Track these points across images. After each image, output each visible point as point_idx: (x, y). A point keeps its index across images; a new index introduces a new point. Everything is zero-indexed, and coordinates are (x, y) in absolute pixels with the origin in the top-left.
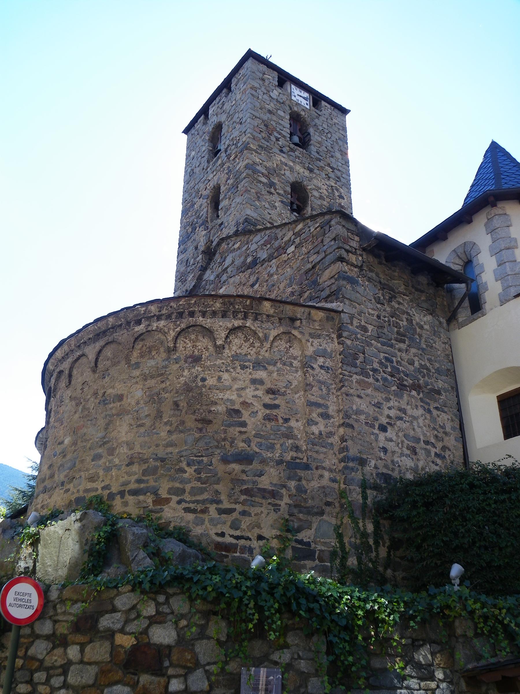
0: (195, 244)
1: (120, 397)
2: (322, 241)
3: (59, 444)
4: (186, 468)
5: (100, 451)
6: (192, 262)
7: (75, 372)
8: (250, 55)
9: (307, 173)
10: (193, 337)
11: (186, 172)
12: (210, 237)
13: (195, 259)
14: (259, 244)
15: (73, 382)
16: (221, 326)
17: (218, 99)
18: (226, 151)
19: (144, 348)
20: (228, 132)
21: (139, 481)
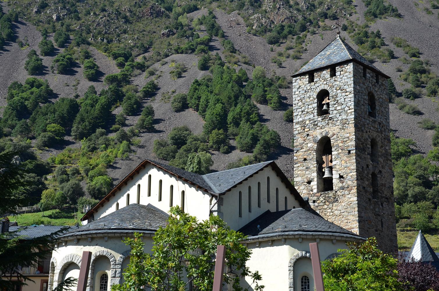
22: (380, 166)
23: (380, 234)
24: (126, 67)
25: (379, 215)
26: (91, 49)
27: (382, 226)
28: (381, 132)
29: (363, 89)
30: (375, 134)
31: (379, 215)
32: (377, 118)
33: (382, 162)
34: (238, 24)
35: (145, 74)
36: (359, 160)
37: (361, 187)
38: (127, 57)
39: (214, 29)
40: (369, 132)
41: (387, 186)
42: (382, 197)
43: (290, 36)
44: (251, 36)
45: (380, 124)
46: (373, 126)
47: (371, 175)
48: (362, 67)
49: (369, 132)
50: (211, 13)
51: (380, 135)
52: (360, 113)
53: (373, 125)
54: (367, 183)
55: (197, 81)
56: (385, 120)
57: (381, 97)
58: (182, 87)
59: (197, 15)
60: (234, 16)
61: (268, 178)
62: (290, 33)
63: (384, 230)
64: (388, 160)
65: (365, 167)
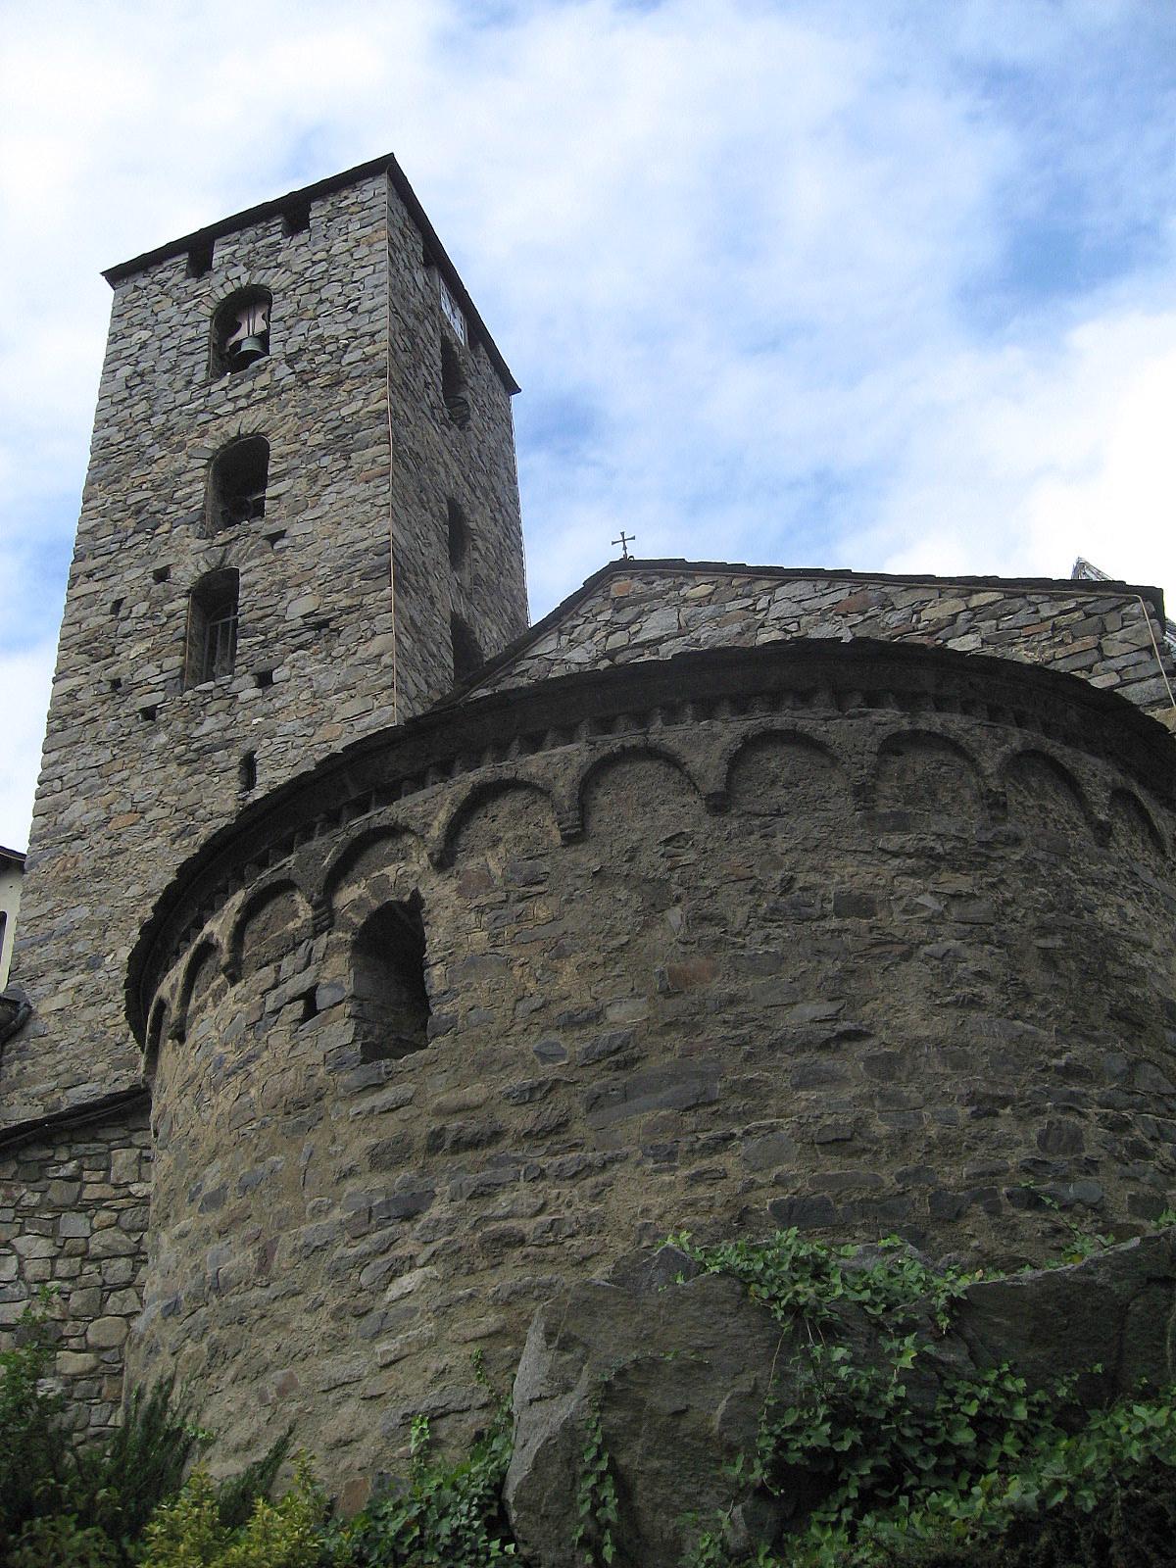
0: (159, 565)
1: (858, 905)
2: (1099, 648)
3: (571, 1022)
4: (1151, 1145)
5: (826, 1061)
6: (142, 608)
7: (602, 798)
8: (387, 166)
9: (467, 490)
10: (1034, 782)
11: (109, 372)
12: (223, 558)
13: (158, 603)
14: (806, 604)
15: (594, 826)
16: (1096, 773)
17: (251, 233)
18: (291, 360)
19: (910, 779)
20: (298, 315)
21: (1032, 1167)
30: (249, 421)
33: (302, 485)
36: (98, 586)
56: (350, 315)
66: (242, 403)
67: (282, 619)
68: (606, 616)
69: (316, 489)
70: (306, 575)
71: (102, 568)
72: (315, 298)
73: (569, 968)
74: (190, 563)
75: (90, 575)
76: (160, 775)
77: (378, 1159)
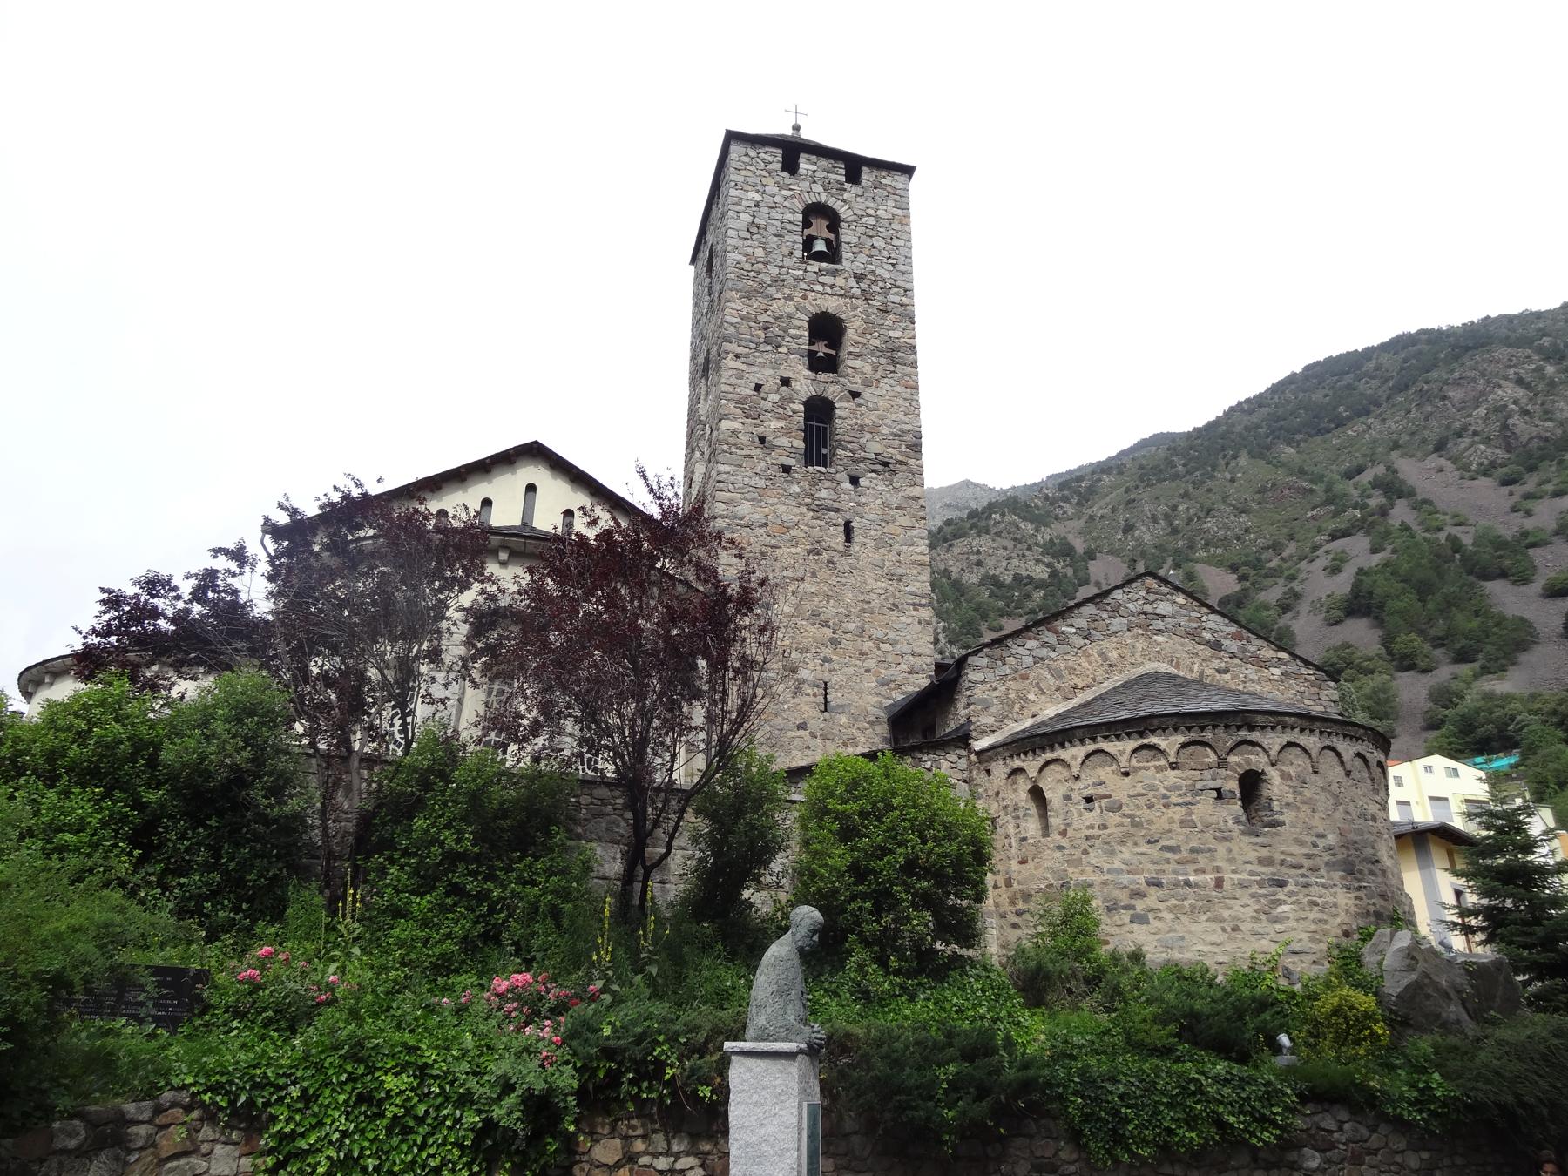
8: (908, 171)
17: (824, 162)
22: (858, 378)
23: (830, 562)
24: (1252, 579)
25: (837, 510)
26: (1199, 568)
27: (848, 538)
28: (867, 296)
29: (777, 199)
30: (831, 305)
31: (837, 510)
32: (845, 263)
33: (868, 369)
34: (1441, 470)
35: (1281, 581)
36: (744, 367)
37: (743, 438)
38: (1257, 564)
39: (1393, 488)
40: (805, 297)
41: (886, 431)
42: (856, 461)
43: (1546, 463)
44: (1467, 483)
45: (859, 277)
46: (823, 285)
47: (805, 404)
48: (779, 152)
49: (805, 297)
50: (1388, 468)
51: (859, 302)
52: (760, 252)
53: (828, 280)
54: (775, 424)
55: (1361, 570)
57: (870, 212)
58: (1342, 585)
59: (1366, 477)
60: (1434, 461)
61: (531, 488)
62: (1542, 459)
63: (855, 547)
64: (895, 363)
65: (771, 384)
66: (828, 290)
67: (863, 448)
68: (1143, 593)
69: (877, 376)
70: (874, 430)
71: (745, 356)
72: (869, 242)
73: (1317, 816)
74: (805, 384)
75: (737, 357)
76: (796, 510)
77: (1261, 861)
